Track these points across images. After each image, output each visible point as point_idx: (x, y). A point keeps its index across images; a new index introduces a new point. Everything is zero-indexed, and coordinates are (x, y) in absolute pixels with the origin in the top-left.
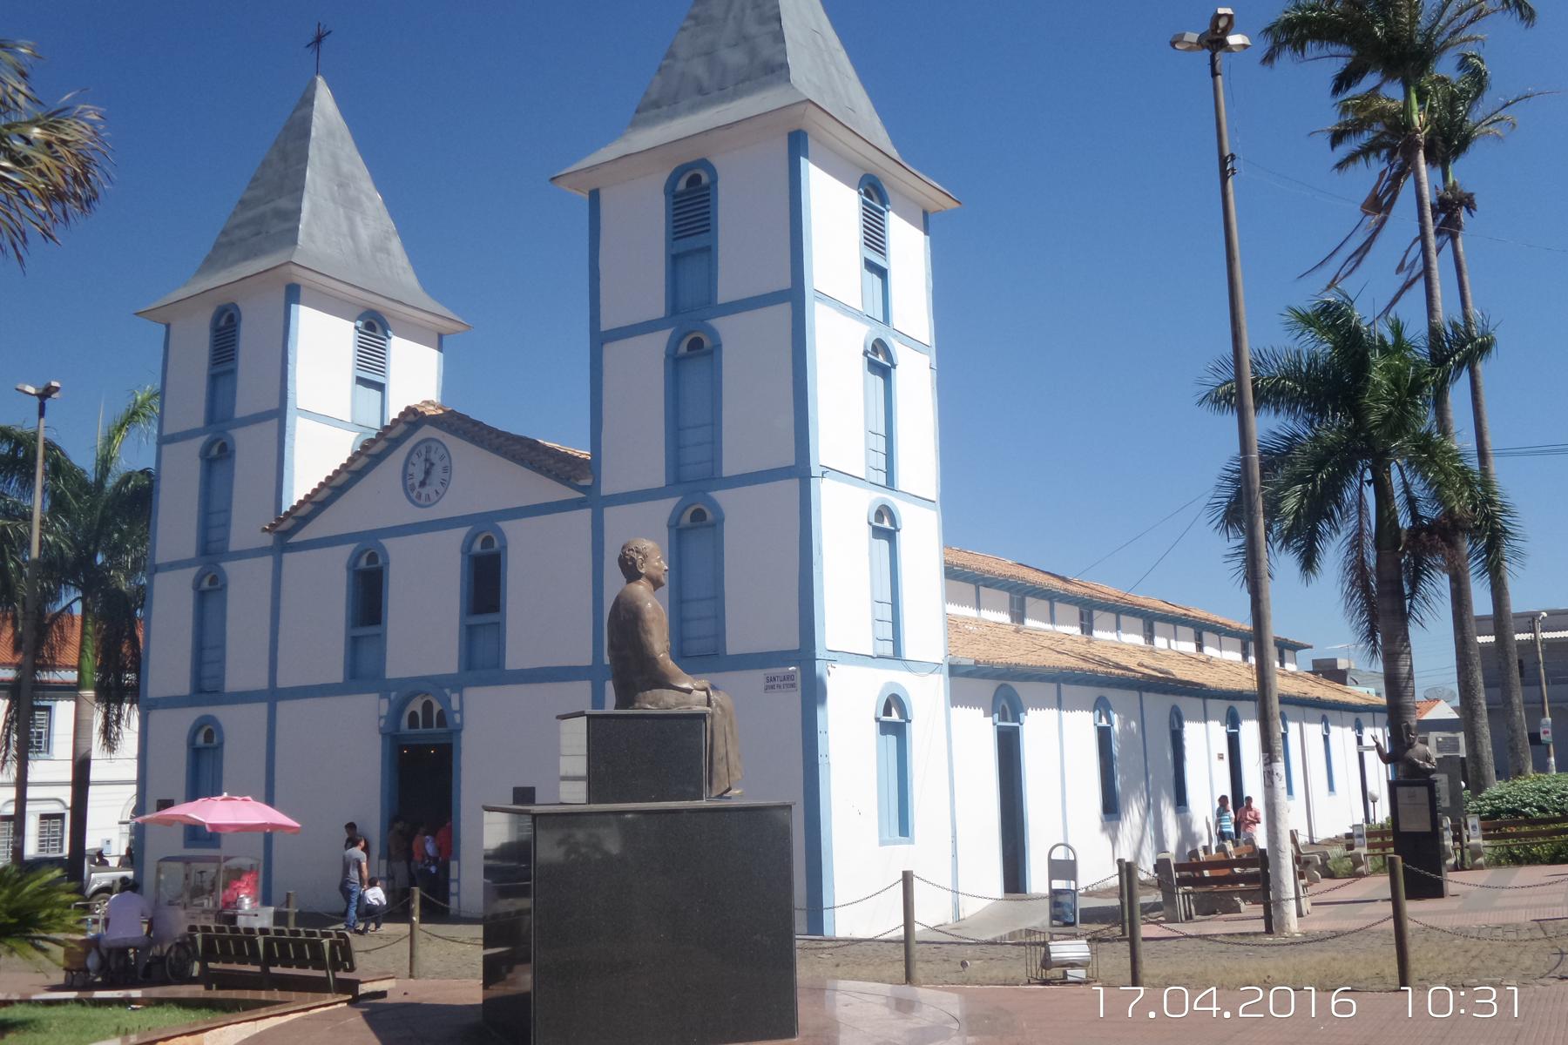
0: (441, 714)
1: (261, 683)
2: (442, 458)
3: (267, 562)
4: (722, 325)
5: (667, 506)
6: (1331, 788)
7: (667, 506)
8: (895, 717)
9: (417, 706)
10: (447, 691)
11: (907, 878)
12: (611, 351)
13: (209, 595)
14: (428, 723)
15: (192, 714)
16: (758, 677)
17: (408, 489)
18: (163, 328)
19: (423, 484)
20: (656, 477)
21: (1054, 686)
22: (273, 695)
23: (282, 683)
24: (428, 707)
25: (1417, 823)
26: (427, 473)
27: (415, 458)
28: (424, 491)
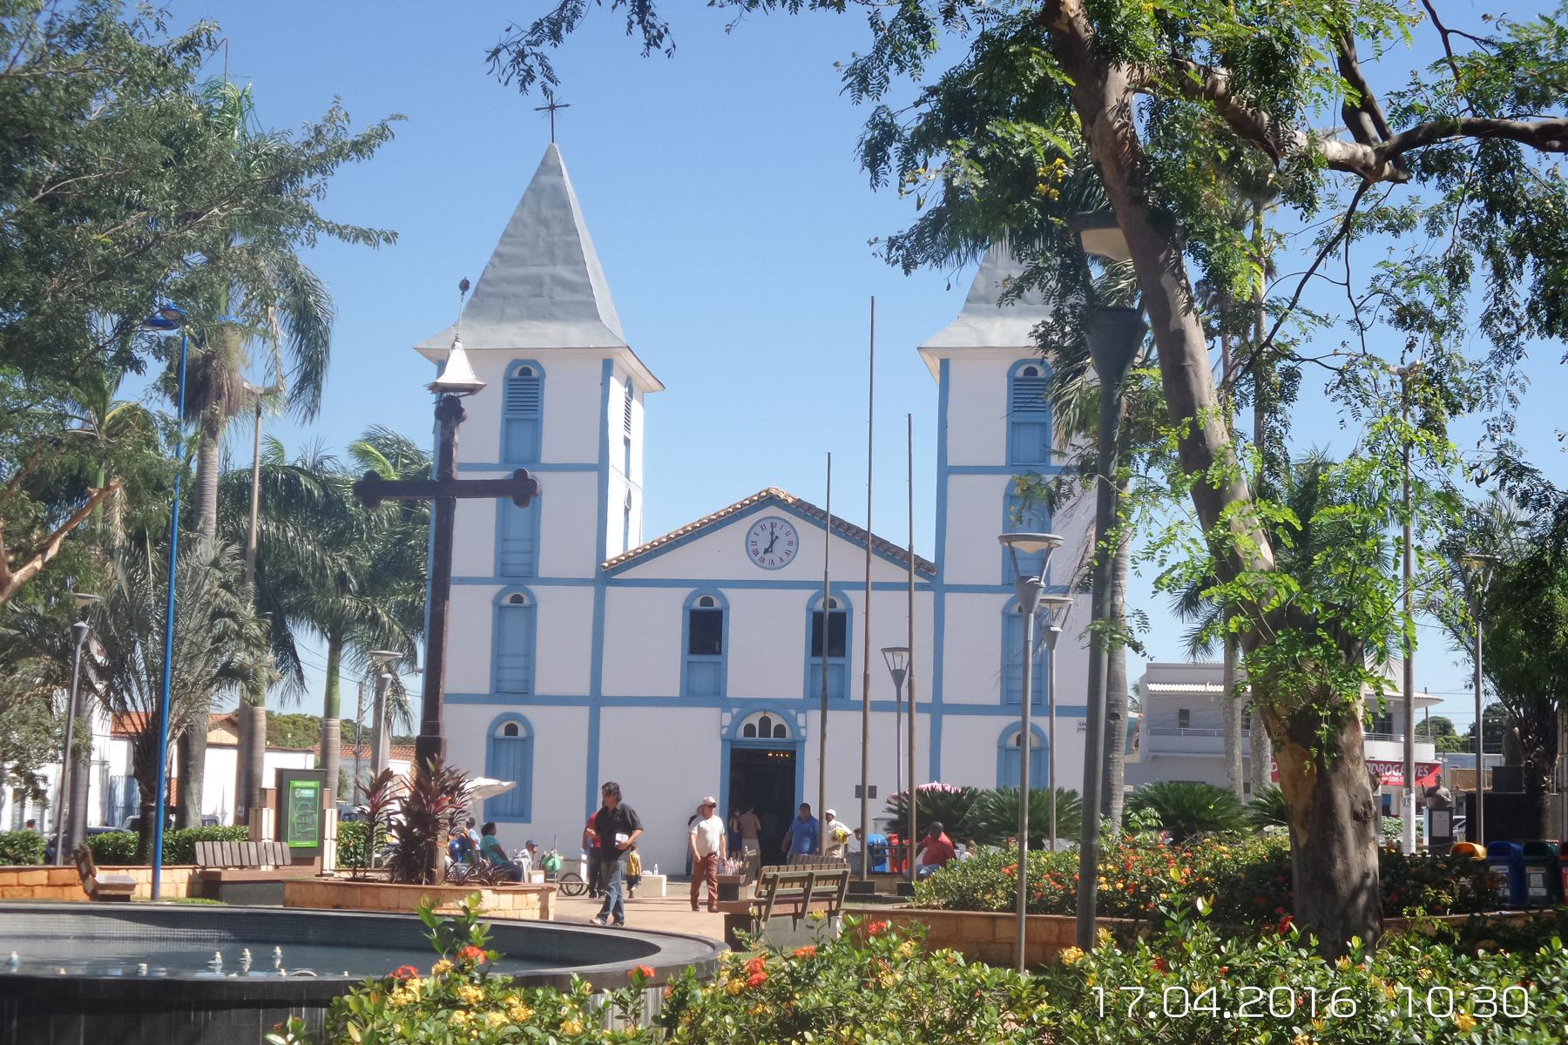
2: (787, 534)
3: (589, 591)
9: (755, 720)
10: (793, 712)
19: (766, 551)
24: (765, 722)
28: (768, 557)
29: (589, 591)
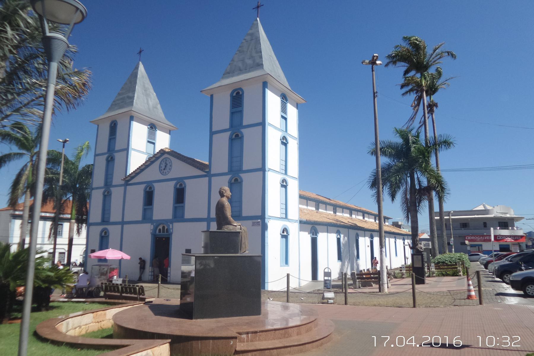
0: (167, 229)
1: (120, 220)
3: (123, 188)
4: (245, 131)
5: (228, 177)
6: (396, 255)
7: (228, 177)
8: (285, 234)
11: (288, 275)
12: (215, 137)
13: (107, 196)
14: (164, 232)
15: (101, 227)
16: (250, 222)
17: (160, 170)
18: (97, 126)
19: (164, 169)
20: (226, 169)
21: (326, 227)
22: (123, 223)
23: (125, 220)
24: (164, 227)
25: (418, 265)
26: (166, 166)
27: (162, 162)
28: (164, 171)
29: (123, 188)
